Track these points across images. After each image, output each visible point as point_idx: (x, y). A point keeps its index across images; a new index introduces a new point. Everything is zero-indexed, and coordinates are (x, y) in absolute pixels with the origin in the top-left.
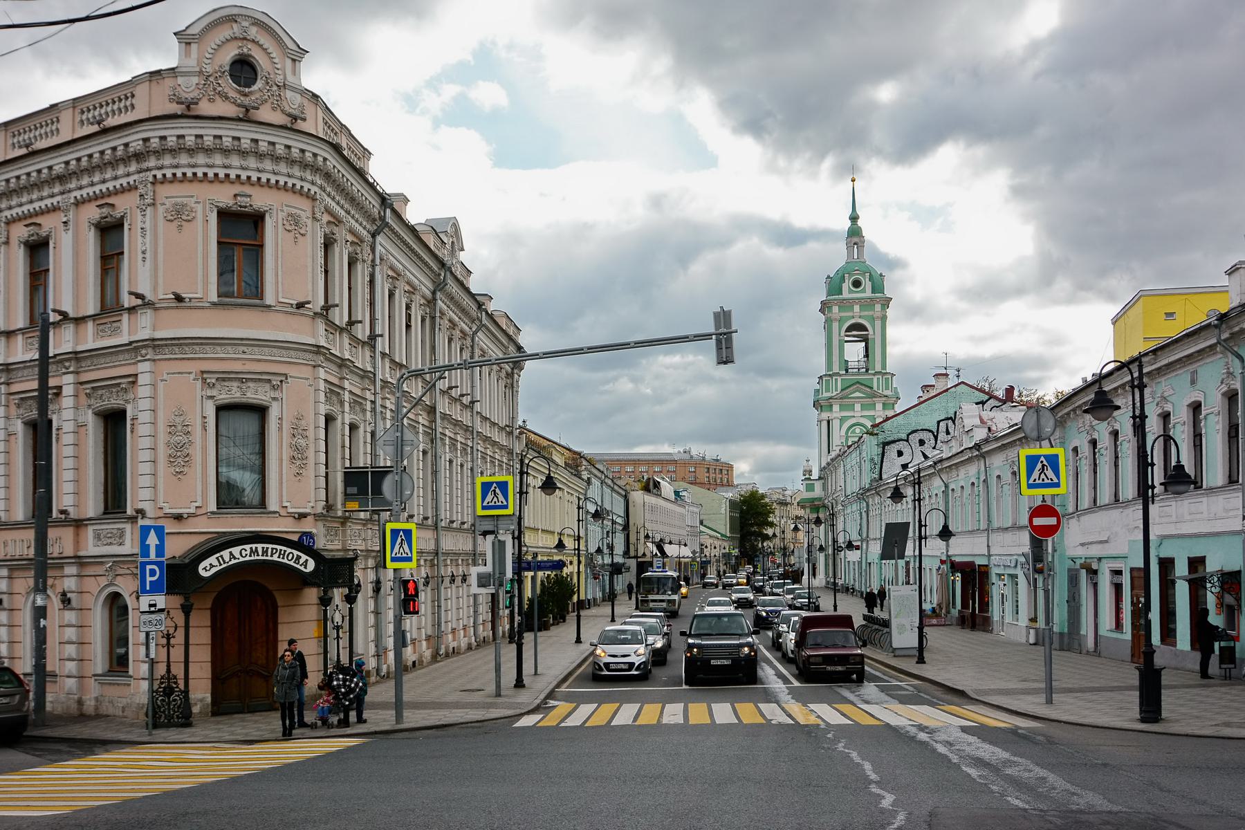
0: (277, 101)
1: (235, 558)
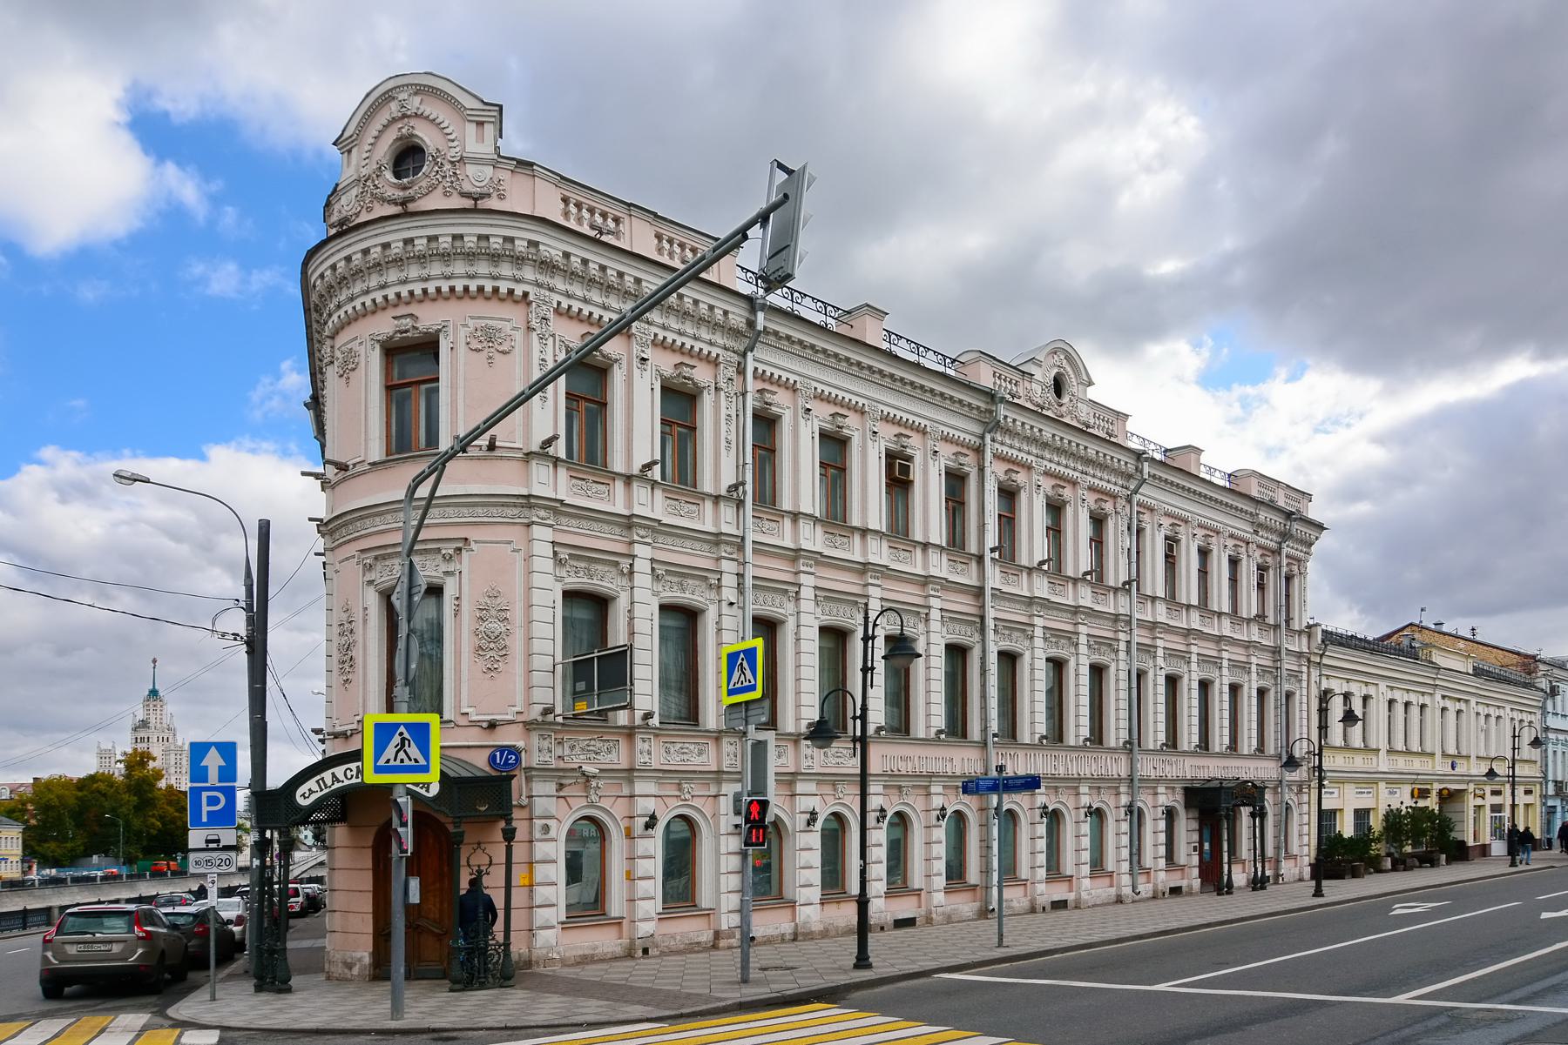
0: (452, 182)
1: (339, 781)
